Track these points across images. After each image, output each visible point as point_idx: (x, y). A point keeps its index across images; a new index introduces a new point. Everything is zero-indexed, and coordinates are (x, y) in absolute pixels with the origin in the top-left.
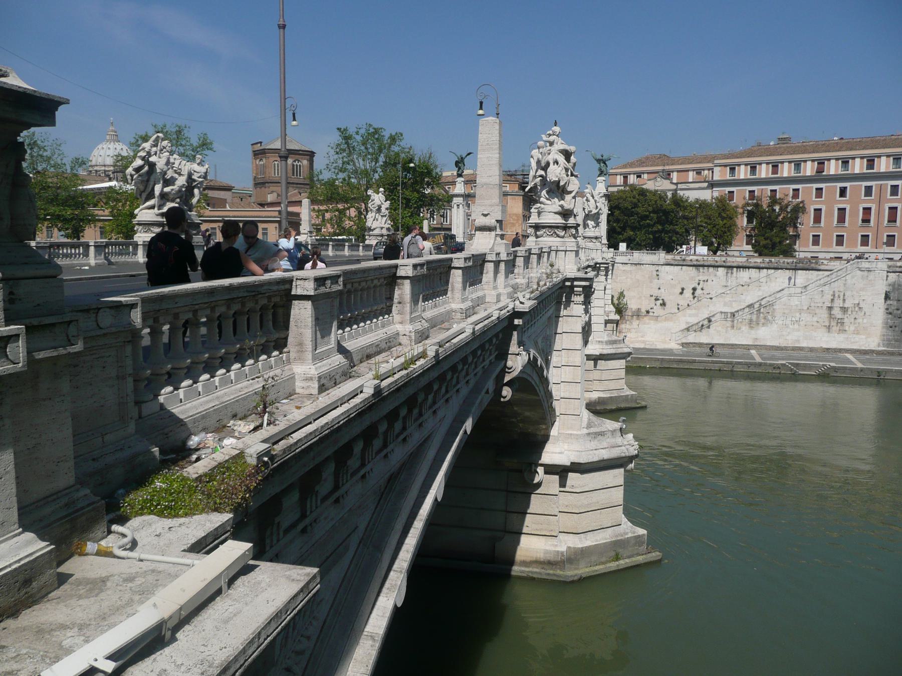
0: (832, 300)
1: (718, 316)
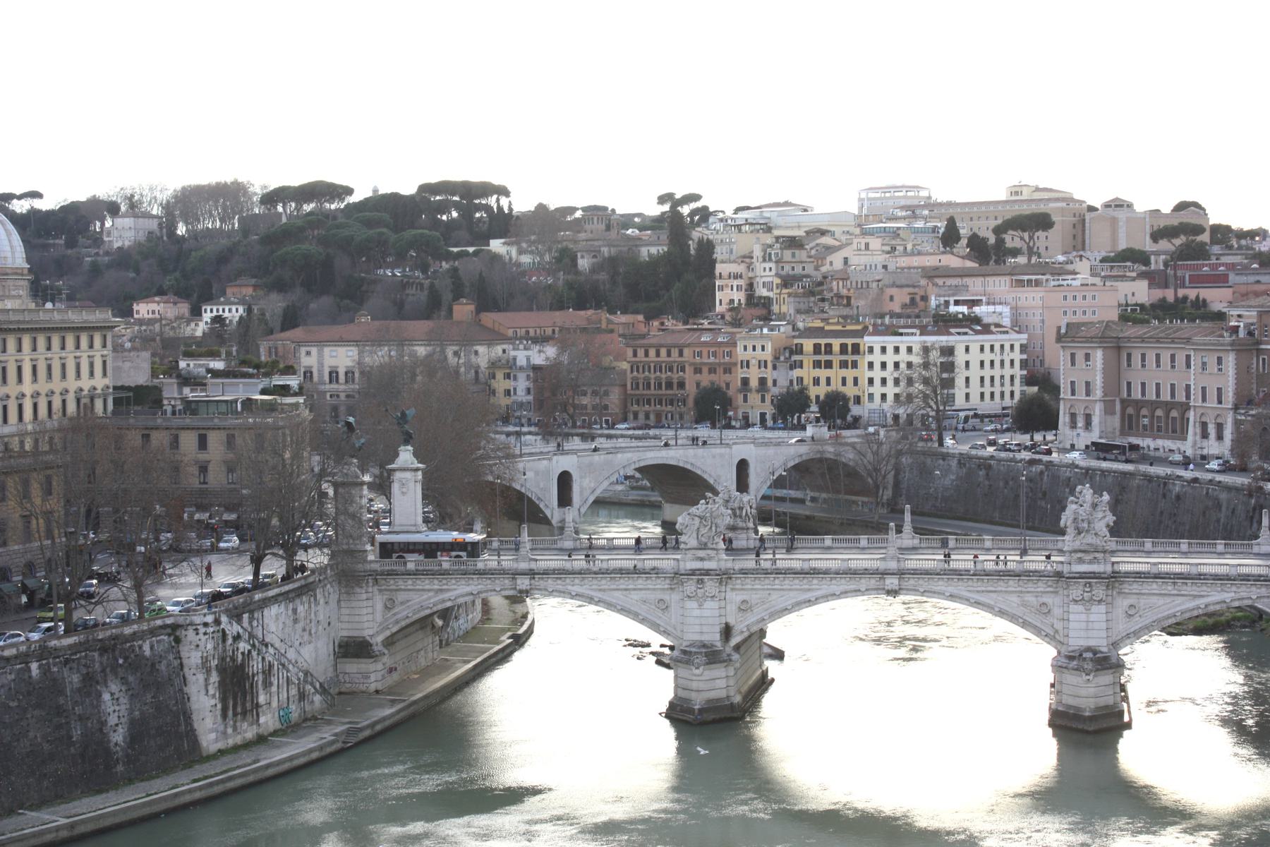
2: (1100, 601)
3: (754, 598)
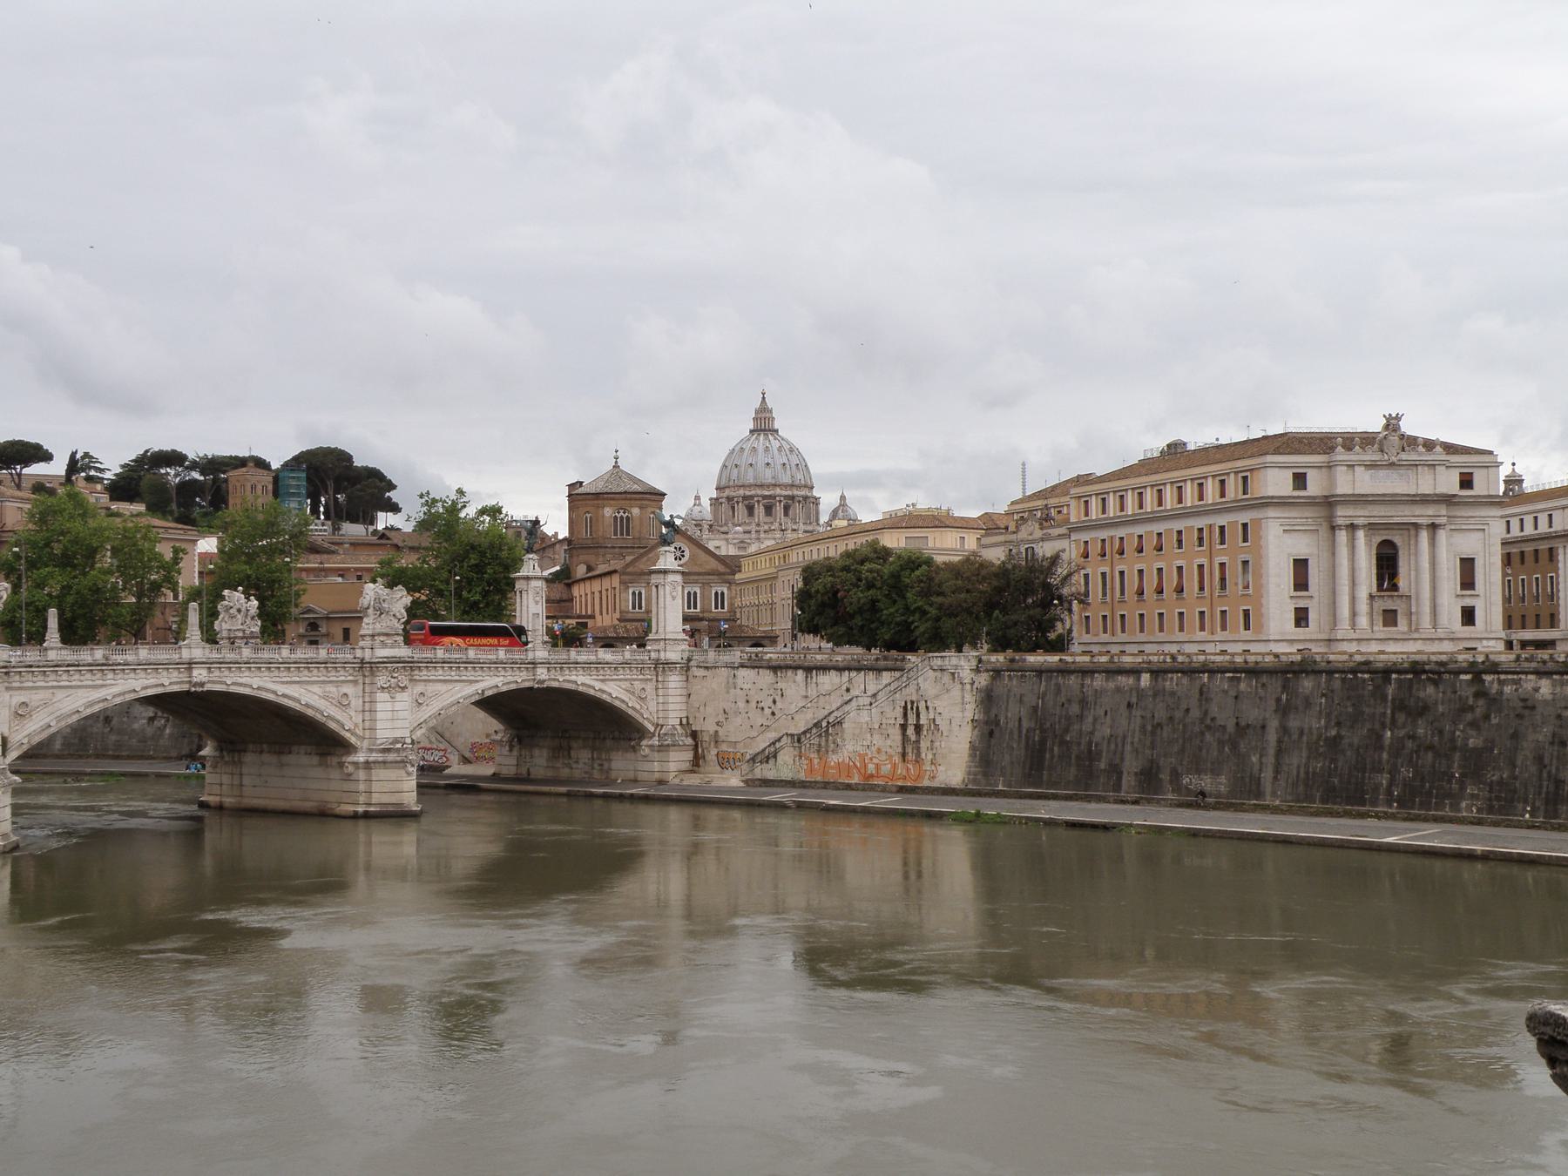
0: (905, 715)
2: (404, 688)
3: (35, 698)
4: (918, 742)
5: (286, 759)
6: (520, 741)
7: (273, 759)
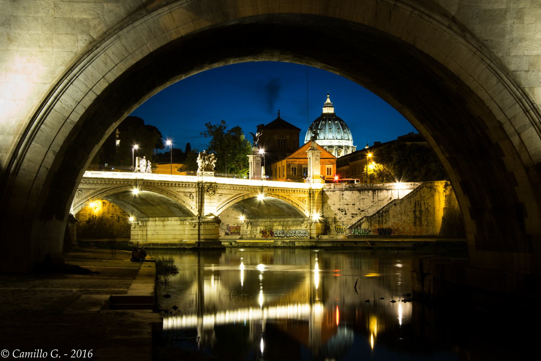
0: (415, 206)
1: (364, 219)
4: (420, 218)
5: (166, 223)
6: (251, 224)
7: (161, 223)
